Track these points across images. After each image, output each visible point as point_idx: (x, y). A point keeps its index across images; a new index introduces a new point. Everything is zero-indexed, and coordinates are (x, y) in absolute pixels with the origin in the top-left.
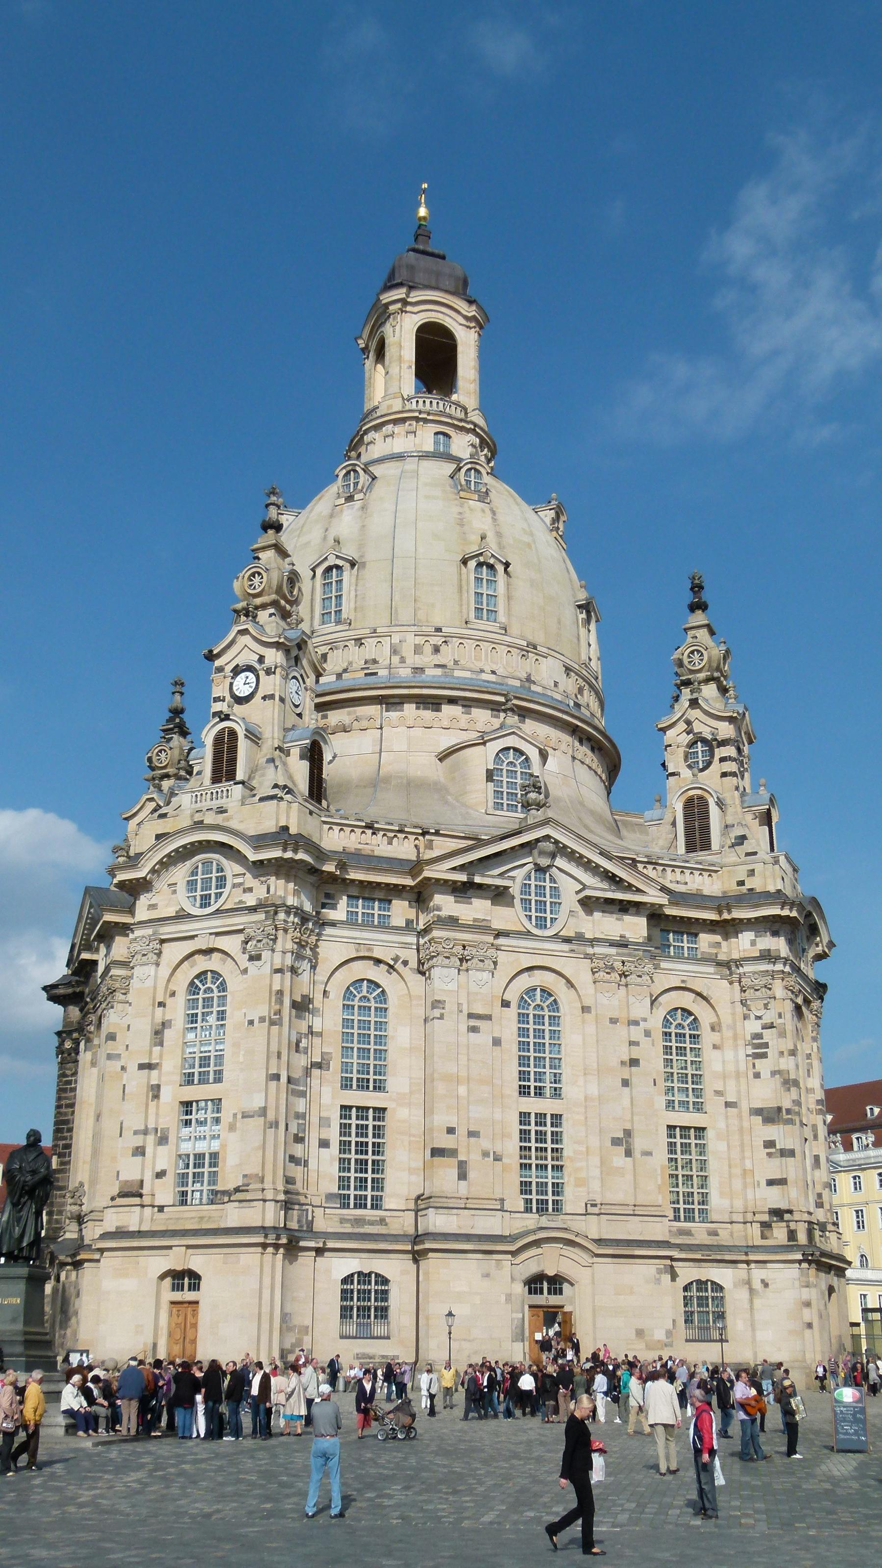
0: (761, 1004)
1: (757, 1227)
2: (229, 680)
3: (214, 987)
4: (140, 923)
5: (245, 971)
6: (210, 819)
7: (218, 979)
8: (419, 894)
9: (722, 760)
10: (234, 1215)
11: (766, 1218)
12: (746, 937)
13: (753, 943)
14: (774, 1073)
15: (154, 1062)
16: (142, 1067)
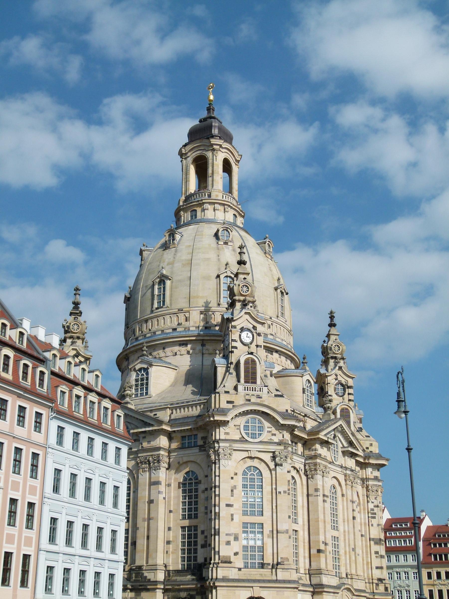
0: (374, 497)
1: (374, 585)
2: (239, 333)
3: (255, 474)
4: (223, 440)
5: (273, 469)
6: (253, 400)
7: (256, 471)
8: (306, 442)
9: (349, 394)
10: (281, 575)
11: (376, 582)
12: (369, 470)
13: (372, 473)
14: (378, 525)
15: (231, 503)
16: (228, 505)
